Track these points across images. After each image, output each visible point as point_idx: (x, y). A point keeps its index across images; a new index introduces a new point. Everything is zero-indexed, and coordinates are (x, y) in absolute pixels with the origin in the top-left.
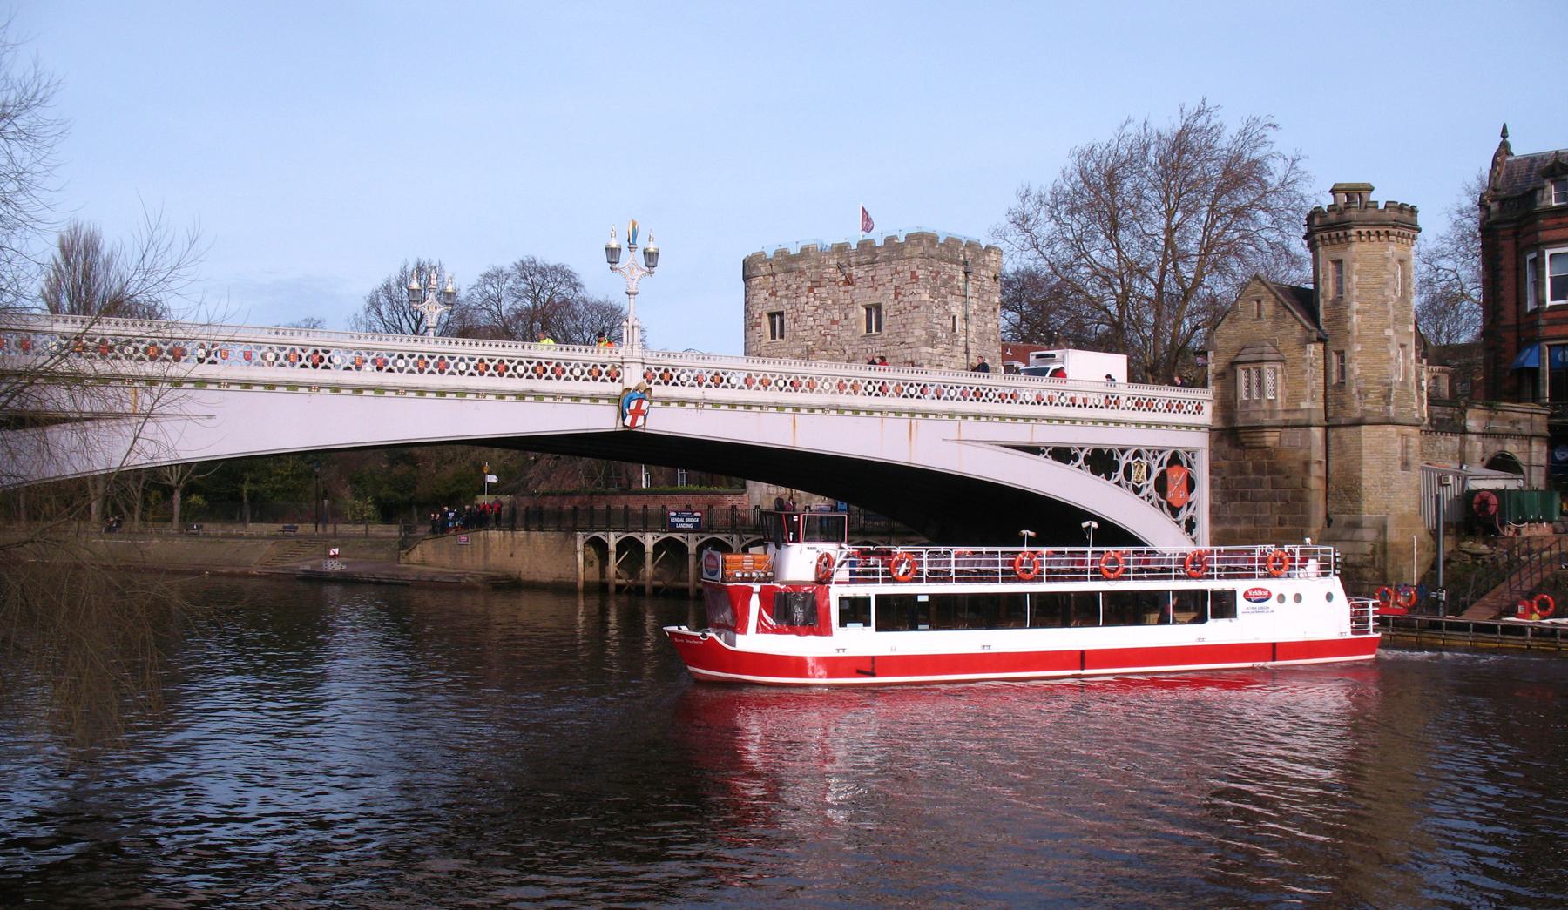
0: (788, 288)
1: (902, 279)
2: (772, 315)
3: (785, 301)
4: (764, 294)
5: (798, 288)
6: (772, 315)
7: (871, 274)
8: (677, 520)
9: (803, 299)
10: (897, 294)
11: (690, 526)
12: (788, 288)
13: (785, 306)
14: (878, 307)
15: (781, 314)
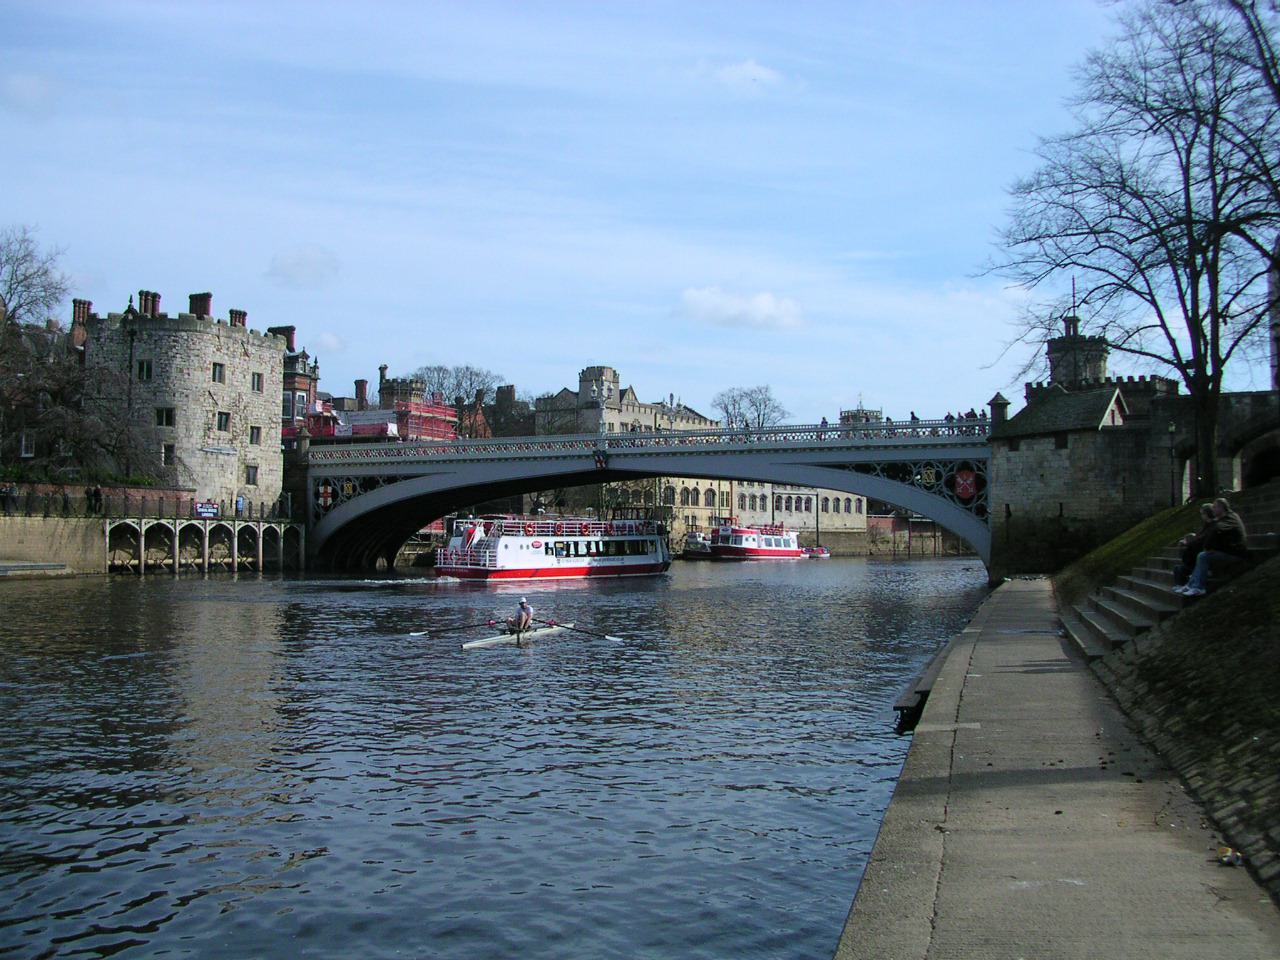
0: (228, 349)
1: (275, 362)
2: (215, 364)
3: (226, 357)
4: (212, 349)
5: (234, 351)
6: (215, 364)
7: (260, 353)
8: (202, 510)
9: (237, 360)
10: (272, 371)
11: (212, 515)
12: (228, 349)
13: (226, 361)
14: (260, 376)
15: (221, 366)
